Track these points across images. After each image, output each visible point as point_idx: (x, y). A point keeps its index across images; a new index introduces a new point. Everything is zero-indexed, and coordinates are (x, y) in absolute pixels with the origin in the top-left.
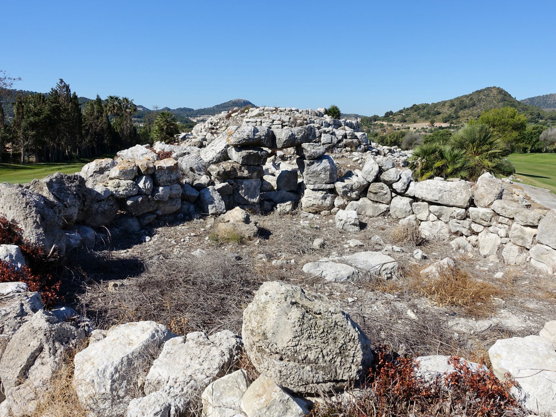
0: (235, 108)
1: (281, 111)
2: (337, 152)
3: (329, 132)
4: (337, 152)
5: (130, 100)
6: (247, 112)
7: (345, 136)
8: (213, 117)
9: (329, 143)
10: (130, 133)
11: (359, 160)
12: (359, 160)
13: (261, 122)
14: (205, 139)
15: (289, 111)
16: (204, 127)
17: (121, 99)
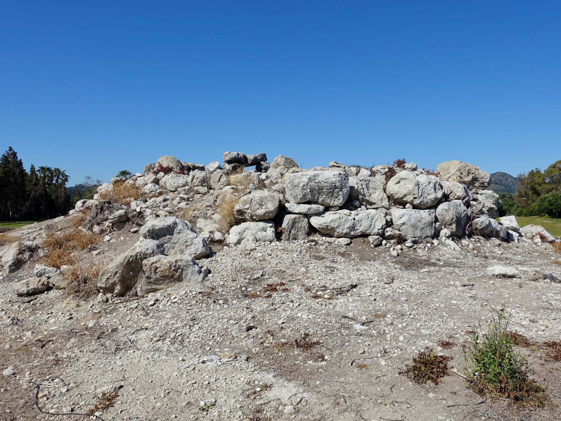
5: (62, 170)
17: (53, 169)
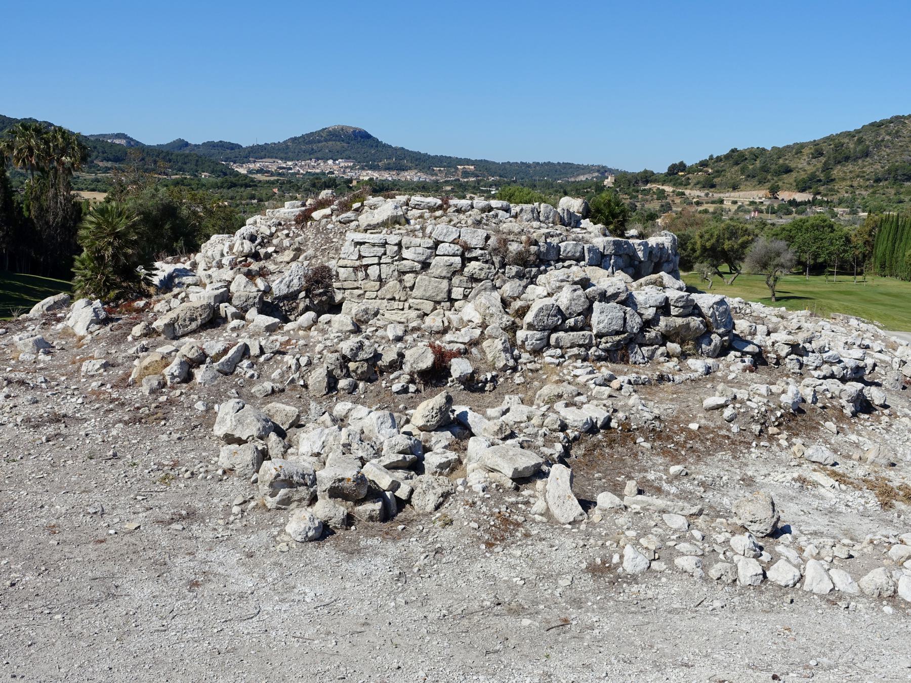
0: (325, 194)
1: (459, 211)
2: (639, 358)
3: (615, 296)
4: (639, 358)
6: (356, 210)
7: (664, 308)
8: (257, 218)
9: (617, 333)
10: (64, 218)
11: (725, 406)
12: (725, 406)
13: (399, 244)
14: (226, 297)
15: (483, 210)
16: (231, 248)
